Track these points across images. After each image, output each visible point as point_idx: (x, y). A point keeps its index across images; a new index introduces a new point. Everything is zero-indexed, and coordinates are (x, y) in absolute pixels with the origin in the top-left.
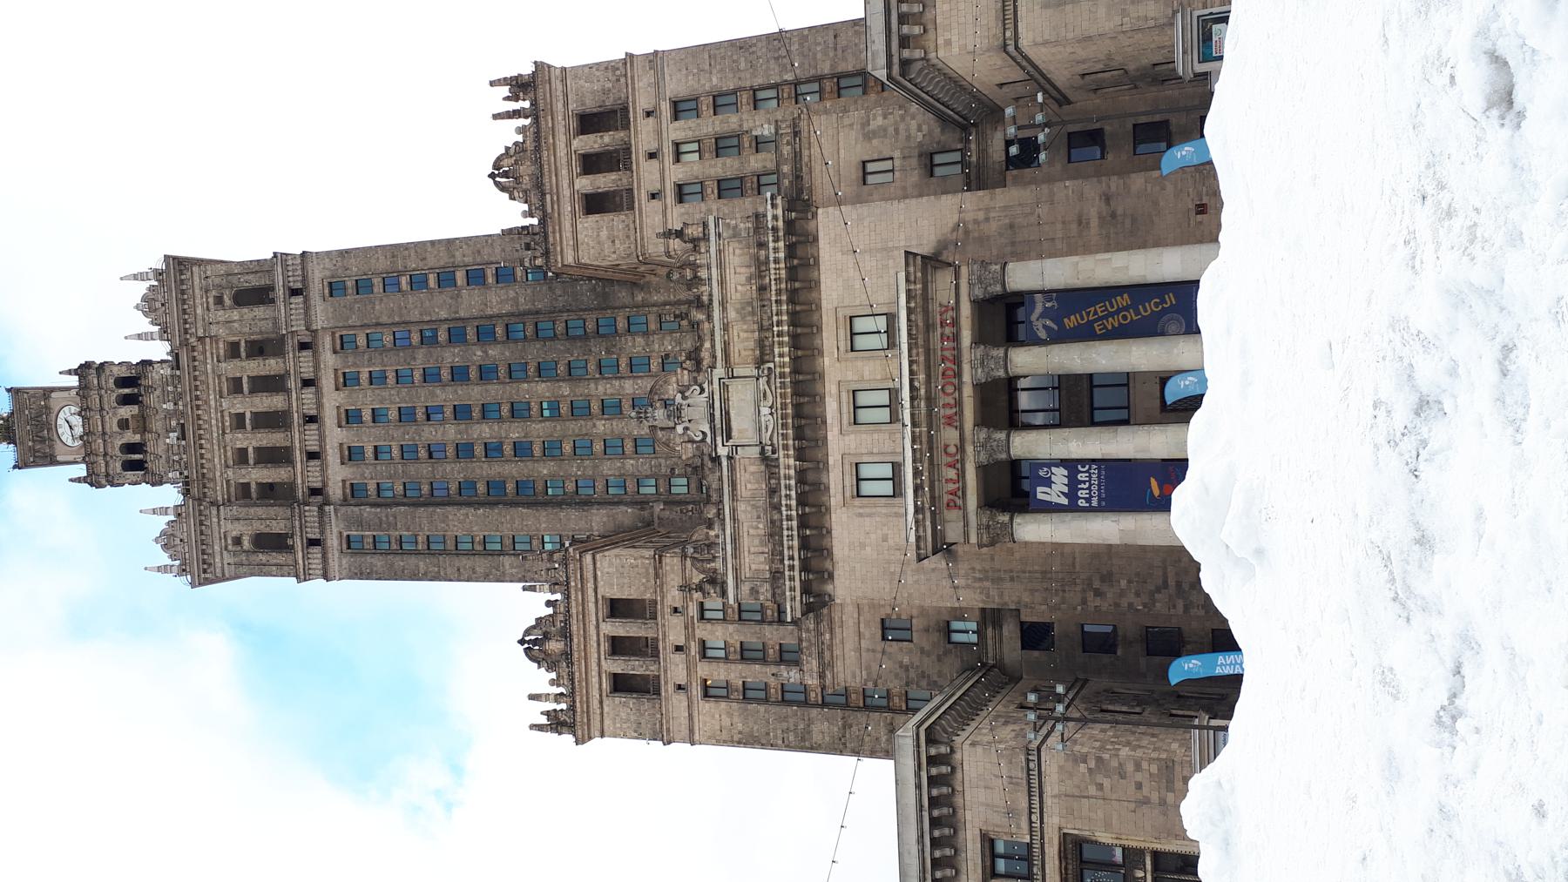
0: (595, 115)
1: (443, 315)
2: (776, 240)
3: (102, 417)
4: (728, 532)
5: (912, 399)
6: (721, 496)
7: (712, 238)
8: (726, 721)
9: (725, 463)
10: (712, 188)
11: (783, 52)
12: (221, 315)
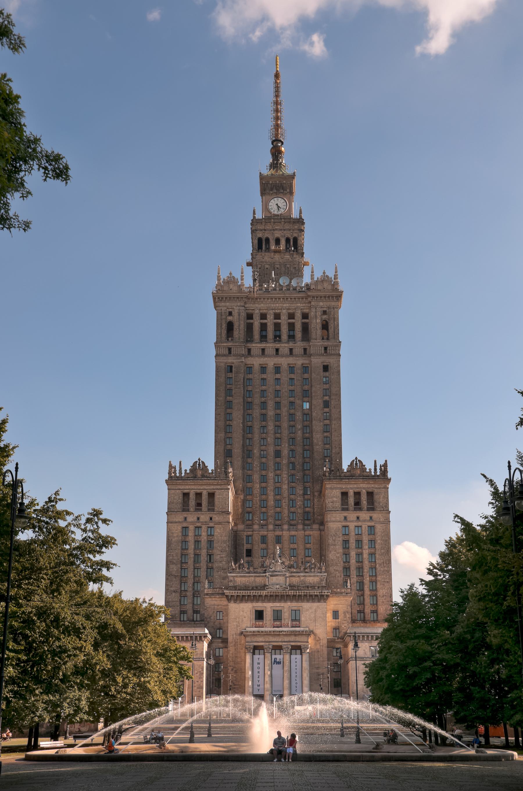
0: (373, 500)
1: (314, 414)
2: (319, 592)
3: (281, 230)
7: (321, 574)
8: (175, 535)
9: (264, 574)
11: (385, 565)
12: (319, 314)
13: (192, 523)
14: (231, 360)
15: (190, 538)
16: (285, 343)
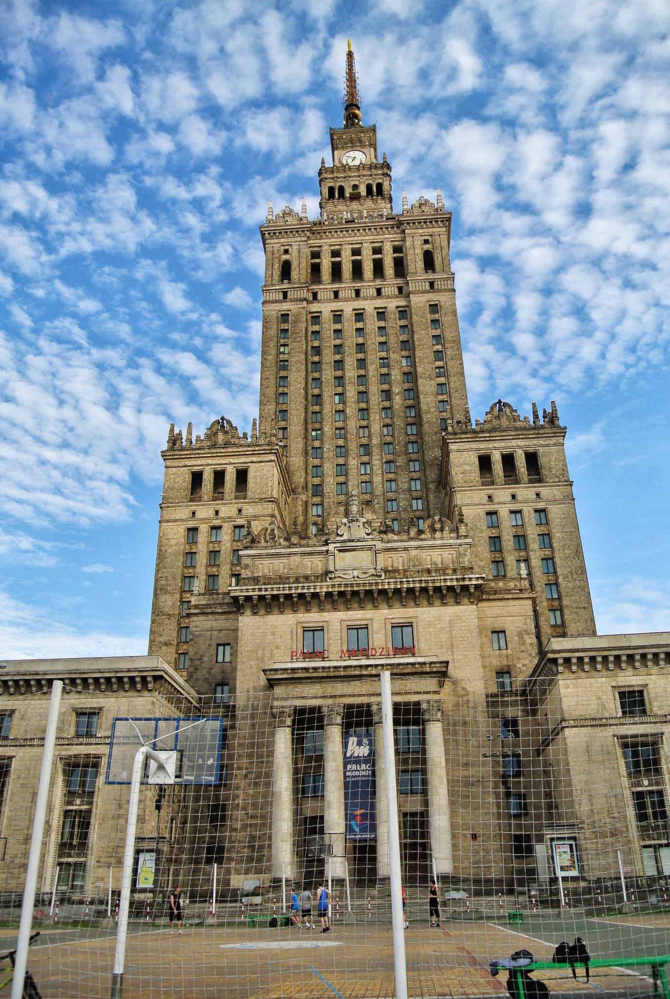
4: (283, 551)
5: (361, 666)
6: (304, 546)
7: (459, 541)
8: (173, 542)
9: (324, 548)
10: (494, 533)
11: (575, 576)
12: (419, 241)
13: (204, 520)
14: (285, 306)
15: (200, 546)
16: (370, 281)
